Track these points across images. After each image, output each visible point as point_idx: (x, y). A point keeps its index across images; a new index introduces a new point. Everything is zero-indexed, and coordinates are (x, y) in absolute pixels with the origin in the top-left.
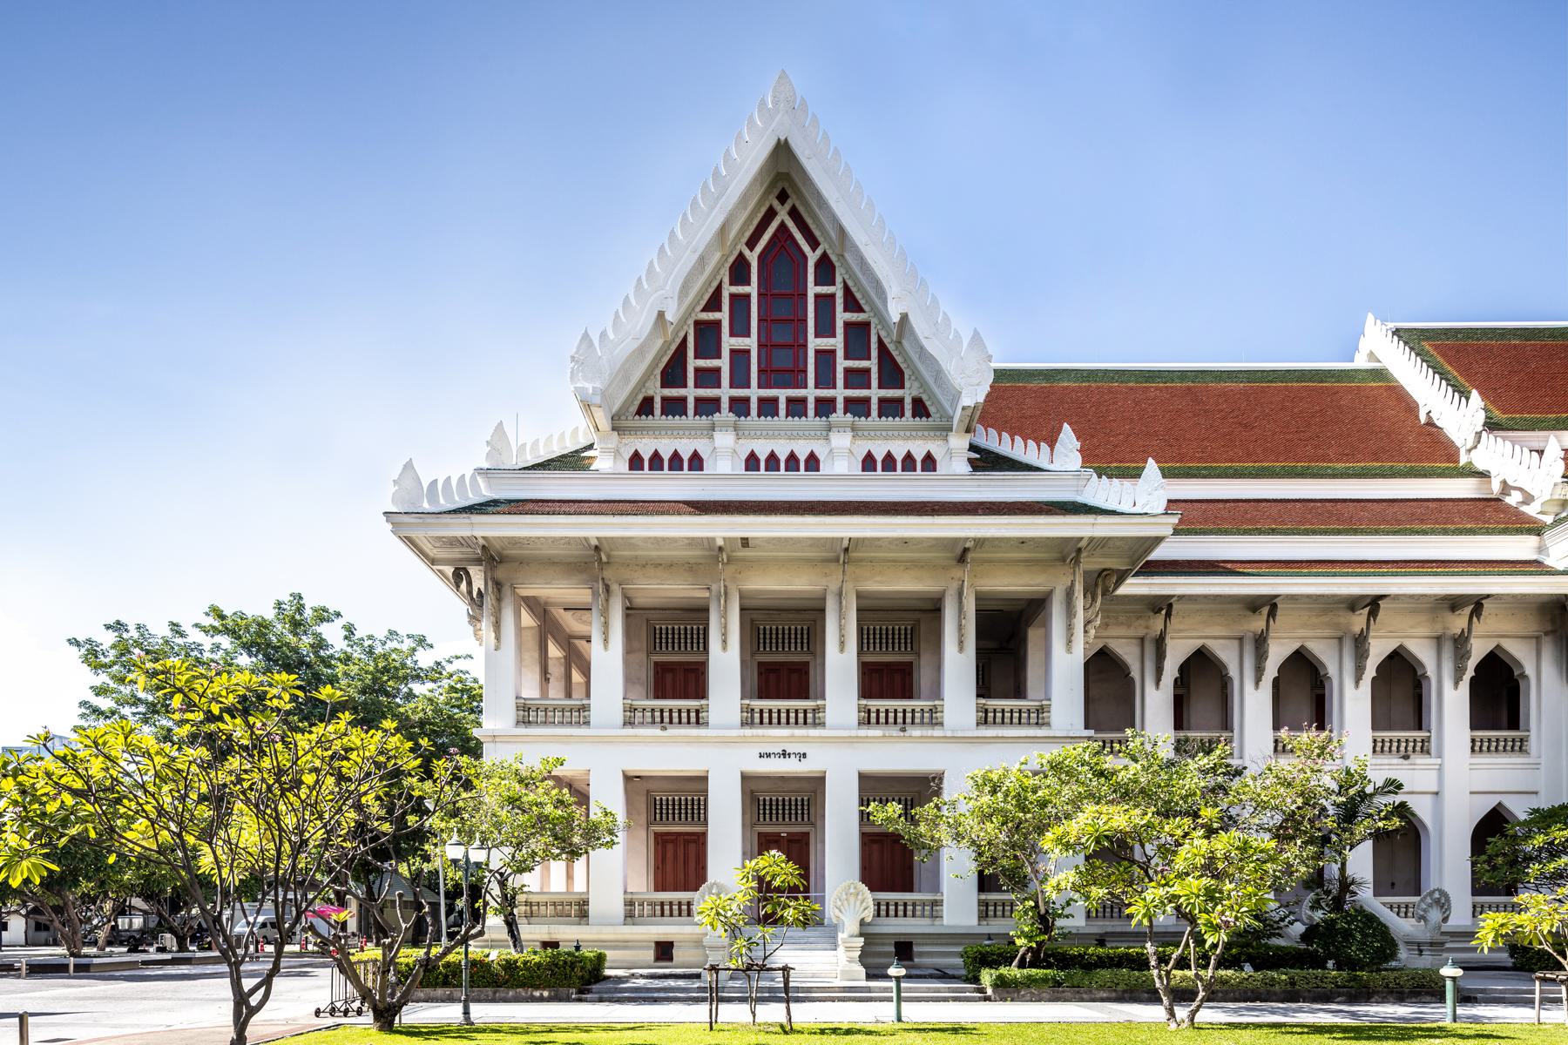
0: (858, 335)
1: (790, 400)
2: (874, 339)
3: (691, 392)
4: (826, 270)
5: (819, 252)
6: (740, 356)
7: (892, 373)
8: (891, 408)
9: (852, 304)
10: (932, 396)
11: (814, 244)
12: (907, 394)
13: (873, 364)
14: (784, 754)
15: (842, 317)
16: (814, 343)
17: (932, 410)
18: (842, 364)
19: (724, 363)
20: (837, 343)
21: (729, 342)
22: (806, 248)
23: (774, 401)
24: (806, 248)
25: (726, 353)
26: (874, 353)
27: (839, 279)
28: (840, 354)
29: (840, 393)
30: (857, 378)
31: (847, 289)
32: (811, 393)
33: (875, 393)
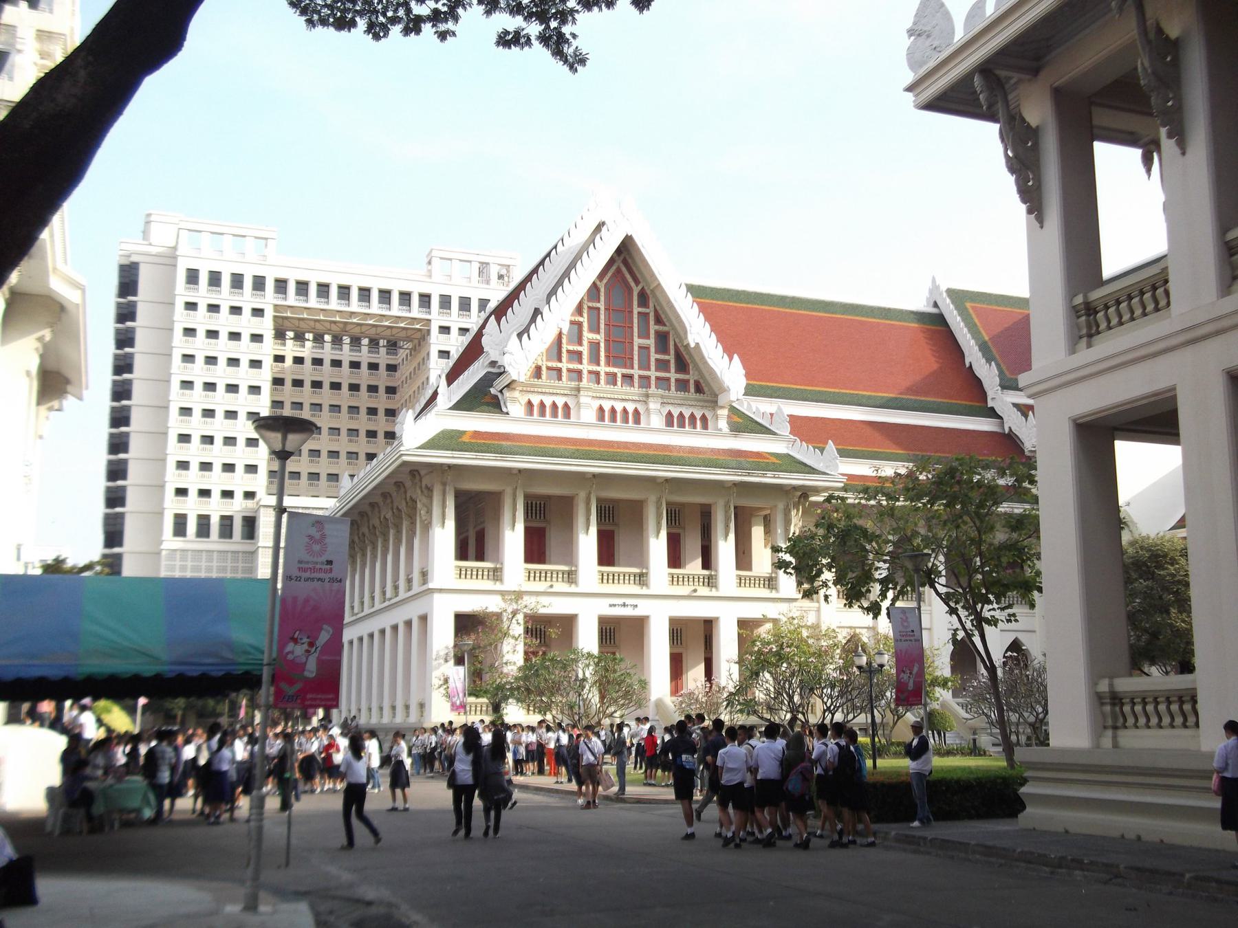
0: (662, 339)
1: (624, 376)
2: (672, 343)
3: (565, 365)
4: (644, 299)
5: (640, 287)
6: (595, 346)
7: (682, 365)
8: (682, 385)
9: (659, 321)
10: (705, 380)
11: (637, 282)
12: (691, 377)
13: (671, 358)
14: (624, 605)
15: (653, 328)
16: (637, 341)
17: (706, 389)
18: (654, 356)
19: (585, 349)
20: (651, 342)
21: (587, 335)
22: (633, 284)
23: (615, 375)
24: (633, 284)
25: (585, 342)
26: (672, 352)
27: (651, 305)
28: (653, 350)
29: (653, 373)
30: (662, 365)
31: (656, 311)
32: (636, 372)
33: (673, 375)
